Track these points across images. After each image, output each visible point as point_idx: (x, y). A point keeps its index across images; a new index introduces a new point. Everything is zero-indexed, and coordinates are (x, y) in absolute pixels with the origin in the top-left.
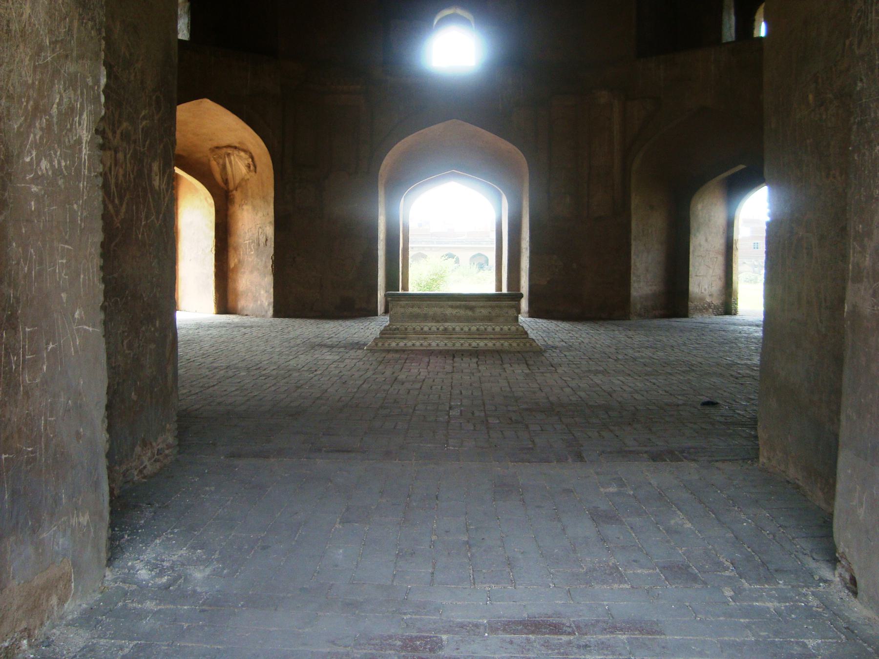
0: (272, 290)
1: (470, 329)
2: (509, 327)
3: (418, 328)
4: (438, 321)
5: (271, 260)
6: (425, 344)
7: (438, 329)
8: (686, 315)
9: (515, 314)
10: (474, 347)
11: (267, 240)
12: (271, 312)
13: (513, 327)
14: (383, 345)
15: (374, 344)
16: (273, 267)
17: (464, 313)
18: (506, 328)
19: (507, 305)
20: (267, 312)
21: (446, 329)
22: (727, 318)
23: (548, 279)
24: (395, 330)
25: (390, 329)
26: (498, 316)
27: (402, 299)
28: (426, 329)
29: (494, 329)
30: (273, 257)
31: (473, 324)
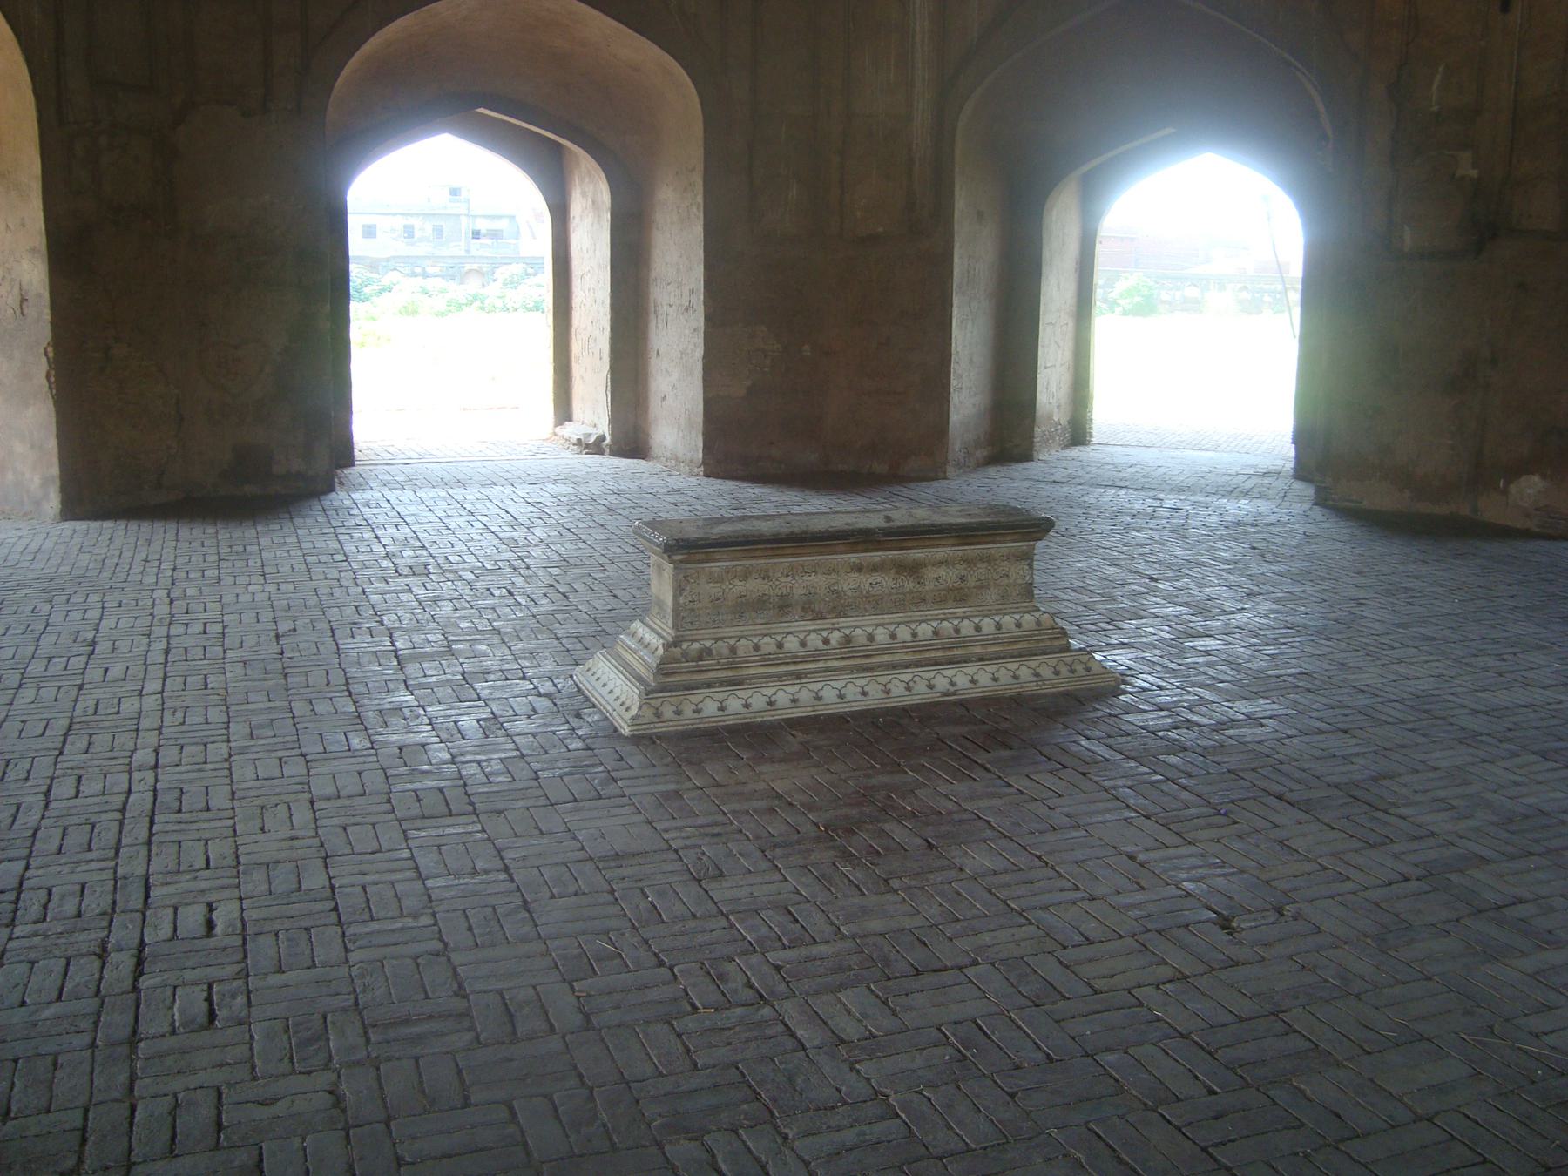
0: (52, 444)
1: (914, 635)
3: (768, 645)
5: (44, 360)
7: (826, 641)
8: (1027, 456)
10: (946, 694)
11: (23, 300)
12: (53, 502)
15: (648, 714)
16: (53, 379)
17: (891, 583)
18: (1008, 621)
20: (38, 503)
21: (848, 640)
22: (1075, 452)
23: (749, 383)
24: (704, 653)
25: (685, 655)
27: (718, 556)
28: (792, 644)
29: (978, 628)
30: (50, 349)
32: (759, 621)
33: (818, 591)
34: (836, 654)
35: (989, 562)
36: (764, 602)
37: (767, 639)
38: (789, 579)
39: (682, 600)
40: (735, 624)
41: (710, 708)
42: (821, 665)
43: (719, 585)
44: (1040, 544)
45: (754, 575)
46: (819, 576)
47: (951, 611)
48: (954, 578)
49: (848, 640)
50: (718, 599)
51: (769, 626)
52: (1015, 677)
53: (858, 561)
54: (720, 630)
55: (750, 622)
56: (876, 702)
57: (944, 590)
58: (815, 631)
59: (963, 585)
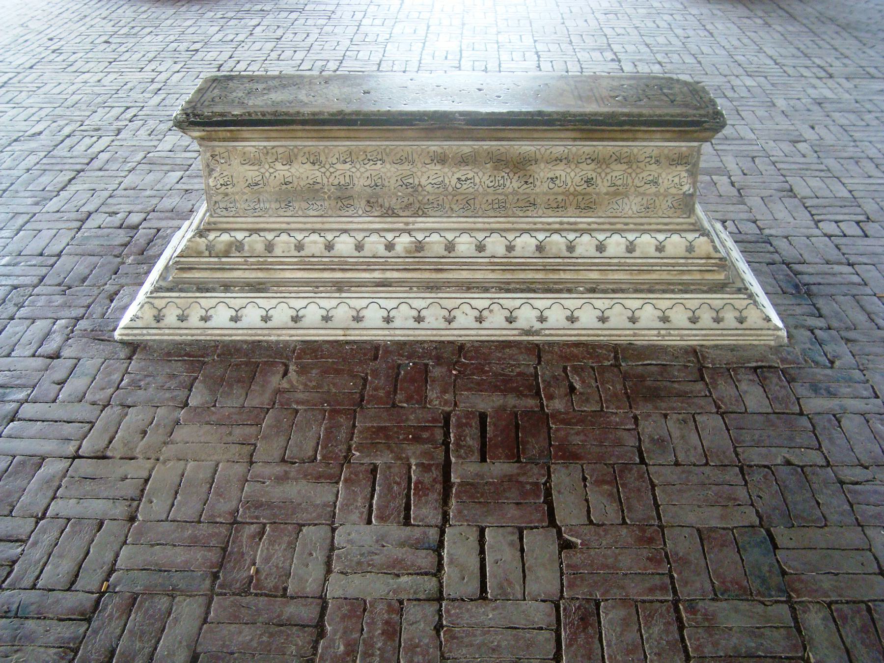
1: (510, 248)
2: (661, 237)
4: (390, 213)
6: (342, 314)
7: (390, 246)
9: (686, 188)
10: (528, 332)
13: (676, 238)
14: (182, 318)
15: (149, 315)
18: (646, 242)
19: (656, 152)
21: (419, 246)
25: (210, 248)
26: (618, 193)
28: (345, 245)
29: (601, 248)
31: (524, 223)
32: (312, 213)
33: (386, 184)
34: (396, 264)
35: (629, 163)
36: (317, 191)
37: (315, 237)
38: (348, 166)
39: (211, 182)
40: (282, 214)
41: (221, 317)
42: (377, 275)
43: (256, 168)
44: (706, 147)
45: (300, 159)
46: (388, 166)
47: (572, 220)
48: (578, 179)
49: (419, 246)
50: (257, 184)
51: (325, 219)
52: (633, 320)
53: (440, 150)
54: (261, 219)
55: (300, 213)
56: (429, 332)
57: (563, 193)
58: (377, 231)
59: (590, 190)
